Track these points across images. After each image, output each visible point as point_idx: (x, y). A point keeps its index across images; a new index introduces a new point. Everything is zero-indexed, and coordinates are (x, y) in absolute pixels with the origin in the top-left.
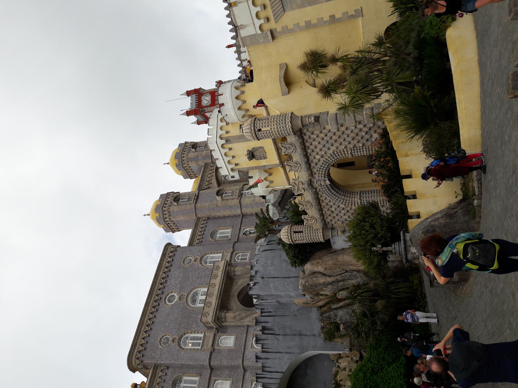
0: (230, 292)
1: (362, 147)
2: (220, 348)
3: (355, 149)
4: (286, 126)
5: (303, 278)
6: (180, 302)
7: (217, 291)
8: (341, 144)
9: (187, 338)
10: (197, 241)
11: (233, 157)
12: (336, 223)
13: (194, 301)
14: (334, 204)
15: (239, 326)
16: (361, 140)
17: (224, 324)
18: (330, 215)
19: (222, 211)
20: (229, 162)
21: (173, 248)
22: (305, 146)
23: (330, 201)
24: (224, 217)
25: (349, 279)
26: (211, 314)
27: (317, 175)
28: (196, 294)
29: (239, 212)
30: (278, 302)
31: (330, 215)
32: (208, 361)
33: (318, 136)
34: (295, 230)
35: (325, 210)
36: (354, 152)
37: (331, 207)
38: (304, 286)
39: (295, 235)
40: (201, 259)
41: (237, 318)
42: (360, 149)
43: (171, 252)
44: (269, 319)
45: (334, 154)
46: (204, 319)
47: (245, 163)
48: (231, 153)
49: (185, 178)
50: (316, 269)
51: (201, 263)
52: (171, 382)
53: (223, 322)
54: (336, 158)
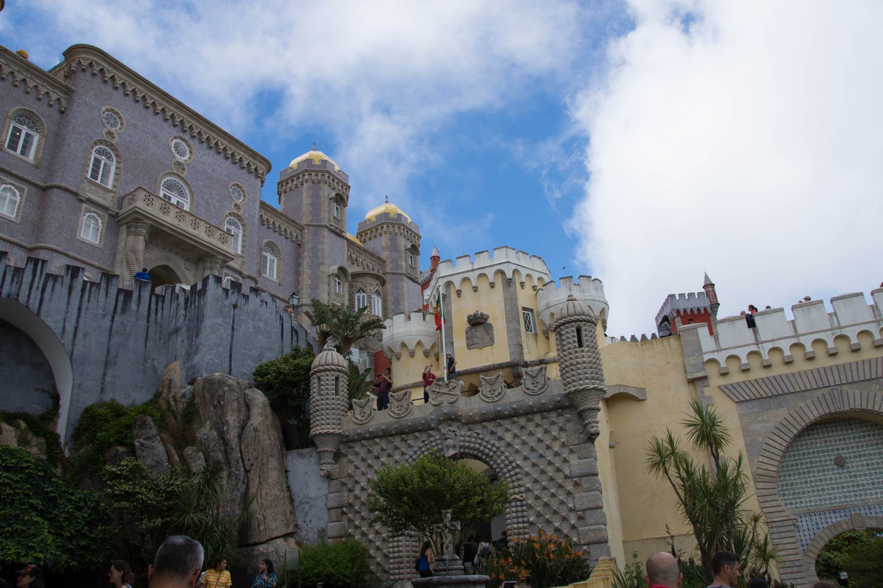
0: (177, 254)
1: (528, 522)
2: (82, 214)
3: (525, 508)
4: (587, 378)
6: (174, 160)
8: (536, 481)
9: (109, 158)
10: (265, 217)
11: (475, 289)
12: (351, 462)
13: (169, 186)
15: (114, 255)
17: (124, 229)
18: (369, 452)
19: (310, 272)
20: (466, 280)
21: (263, 174)
22: (534, 413)
23: (403, 454)
24: (297, 273)
25: (229, 475)
26: (149, 209)
28: (181, 194)
30: (177, 330)
32: (63, 184)
33: (555, 439)
34: (341, 379)
36: (516, 506)
37: (389, 456)
38: (221, 383)
39: (331, 377)
41: (132, 257)
44: (144, 309)
45: (514, 468)
46: (141, 195)
47: (461, 311)
48: (484, 286)
51: (230, 214)
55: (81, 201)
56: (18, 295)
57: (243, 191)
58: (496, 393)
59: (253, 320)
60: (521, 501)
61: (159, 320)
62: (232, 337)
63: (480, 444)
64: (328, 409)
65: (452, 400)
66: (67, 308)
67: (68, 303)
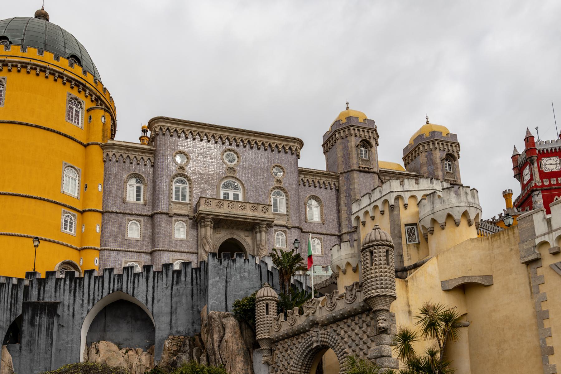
0: (237, 229)
5: (219, 316)
7: (236, 213)
10: (305, 180)
13: (227, 186)
19: (346, 208)
24: (339, 211)
28: (236, 188)
31: (284, 347)
34: (270, 304)
40: (280, 188)
41: (204, 241)
44: (189, 279)
46: (203, 201)
49: (405, 150)
50: (228, 330)
51: (274, 189)
52: (137, 172)
53: (200, 224)
56: (122, 288)
59: (240, 273)
61: (199, 282)
62: (226, 287)
64: (264, 324)
66: (147, 289)
67: (147, 286)
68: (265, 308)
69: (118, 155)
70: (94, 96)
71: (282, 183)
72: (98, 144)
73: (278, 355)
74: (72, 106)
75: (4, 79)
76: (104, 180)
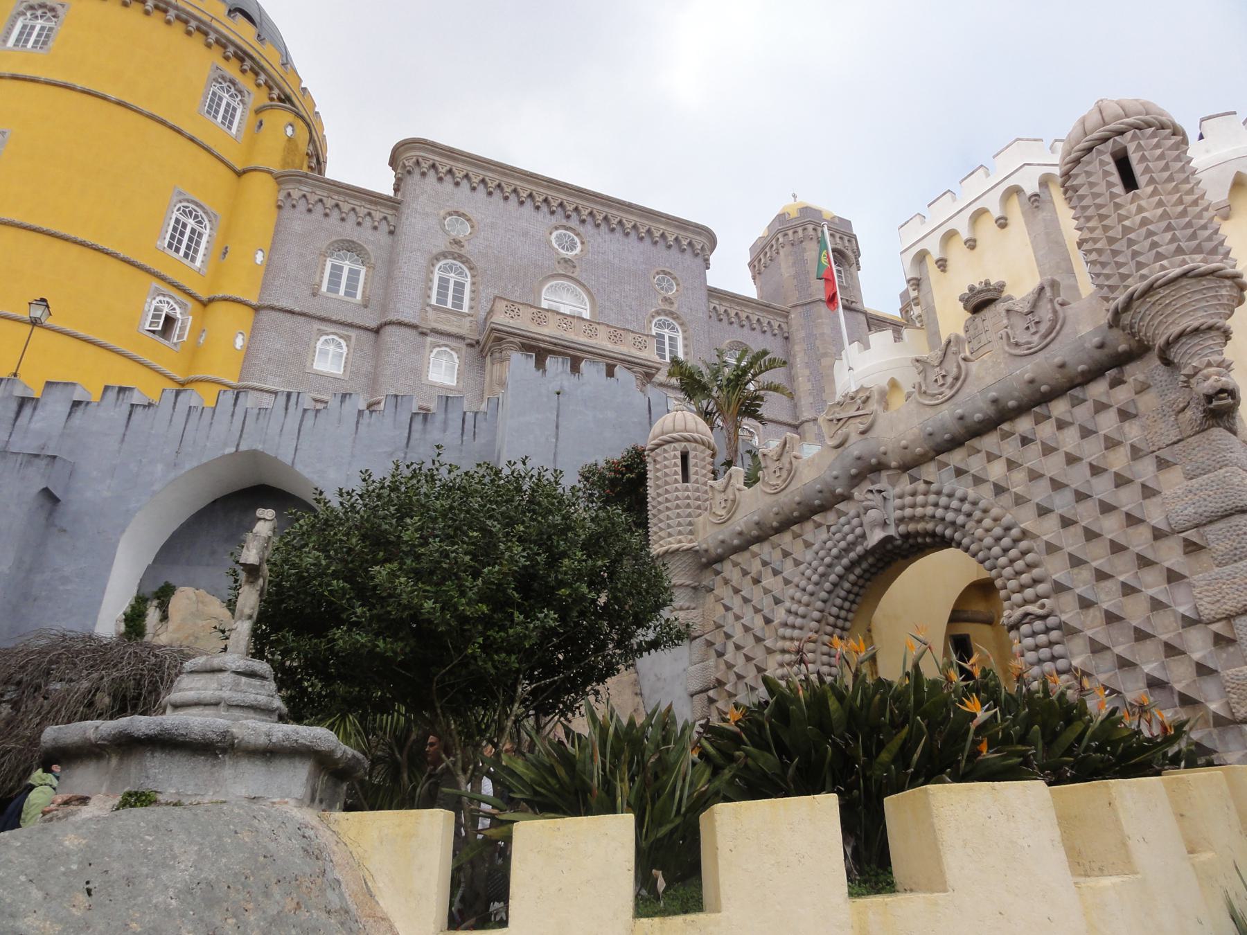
2: (427, 350)
3: (1055, 635)
7: (575, 338)
10: (721, 309)
14: (787, 582)
16: (1107, 661)
17: (488, 359)
18: (745, 573)
19: (807, 372)
21: (703, 249)
23: (797, 563)
27: (909, 488)
29: (806, 415)
31: (745, 573)
33: (1111, 444)
35: (763, 550)
36: (1034, 634)
37: (776, 573)
39: (674, 453)
42: (1053, 659)
43: (690, 244)
45: (1016, 541)
46: (501, 306)
51: (658, 313)
52: (355, 239)
54: (996, 550)
55: (424, 334)
57: (674, 278)
58: (949, 380)
60: (1043, 618)
63: (936, 505)
65: (862, 427)
68: (679, 462)
69: (313, 199)
70: (276, 92)
71: (676, 305)
72: (270, 172)
73: (727, 602)
74: (220, 93)
75: (63, 6)
76: (274, 243)
